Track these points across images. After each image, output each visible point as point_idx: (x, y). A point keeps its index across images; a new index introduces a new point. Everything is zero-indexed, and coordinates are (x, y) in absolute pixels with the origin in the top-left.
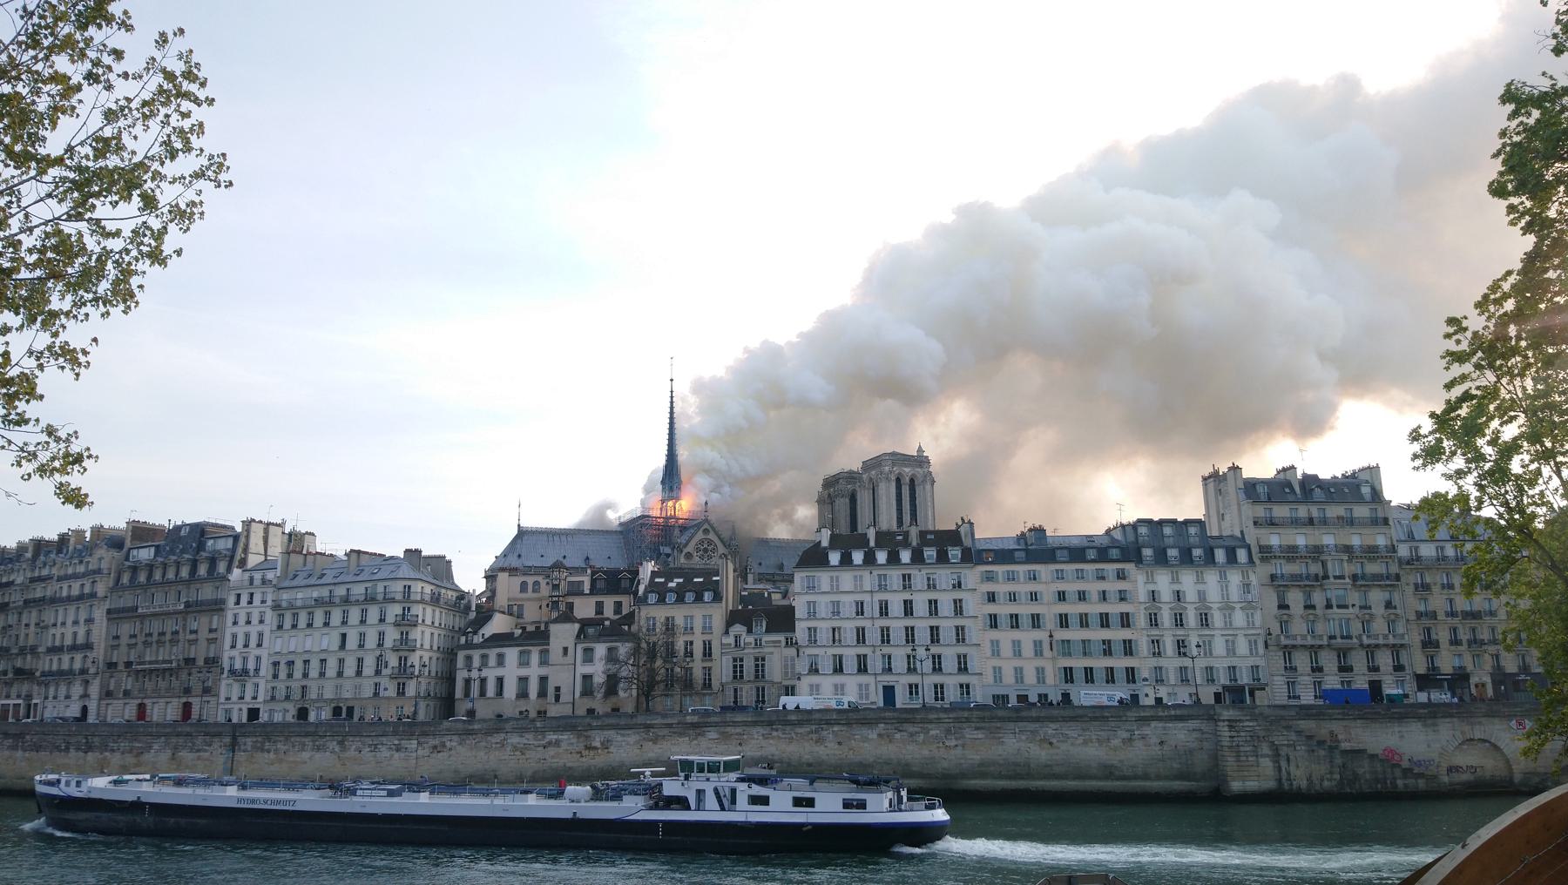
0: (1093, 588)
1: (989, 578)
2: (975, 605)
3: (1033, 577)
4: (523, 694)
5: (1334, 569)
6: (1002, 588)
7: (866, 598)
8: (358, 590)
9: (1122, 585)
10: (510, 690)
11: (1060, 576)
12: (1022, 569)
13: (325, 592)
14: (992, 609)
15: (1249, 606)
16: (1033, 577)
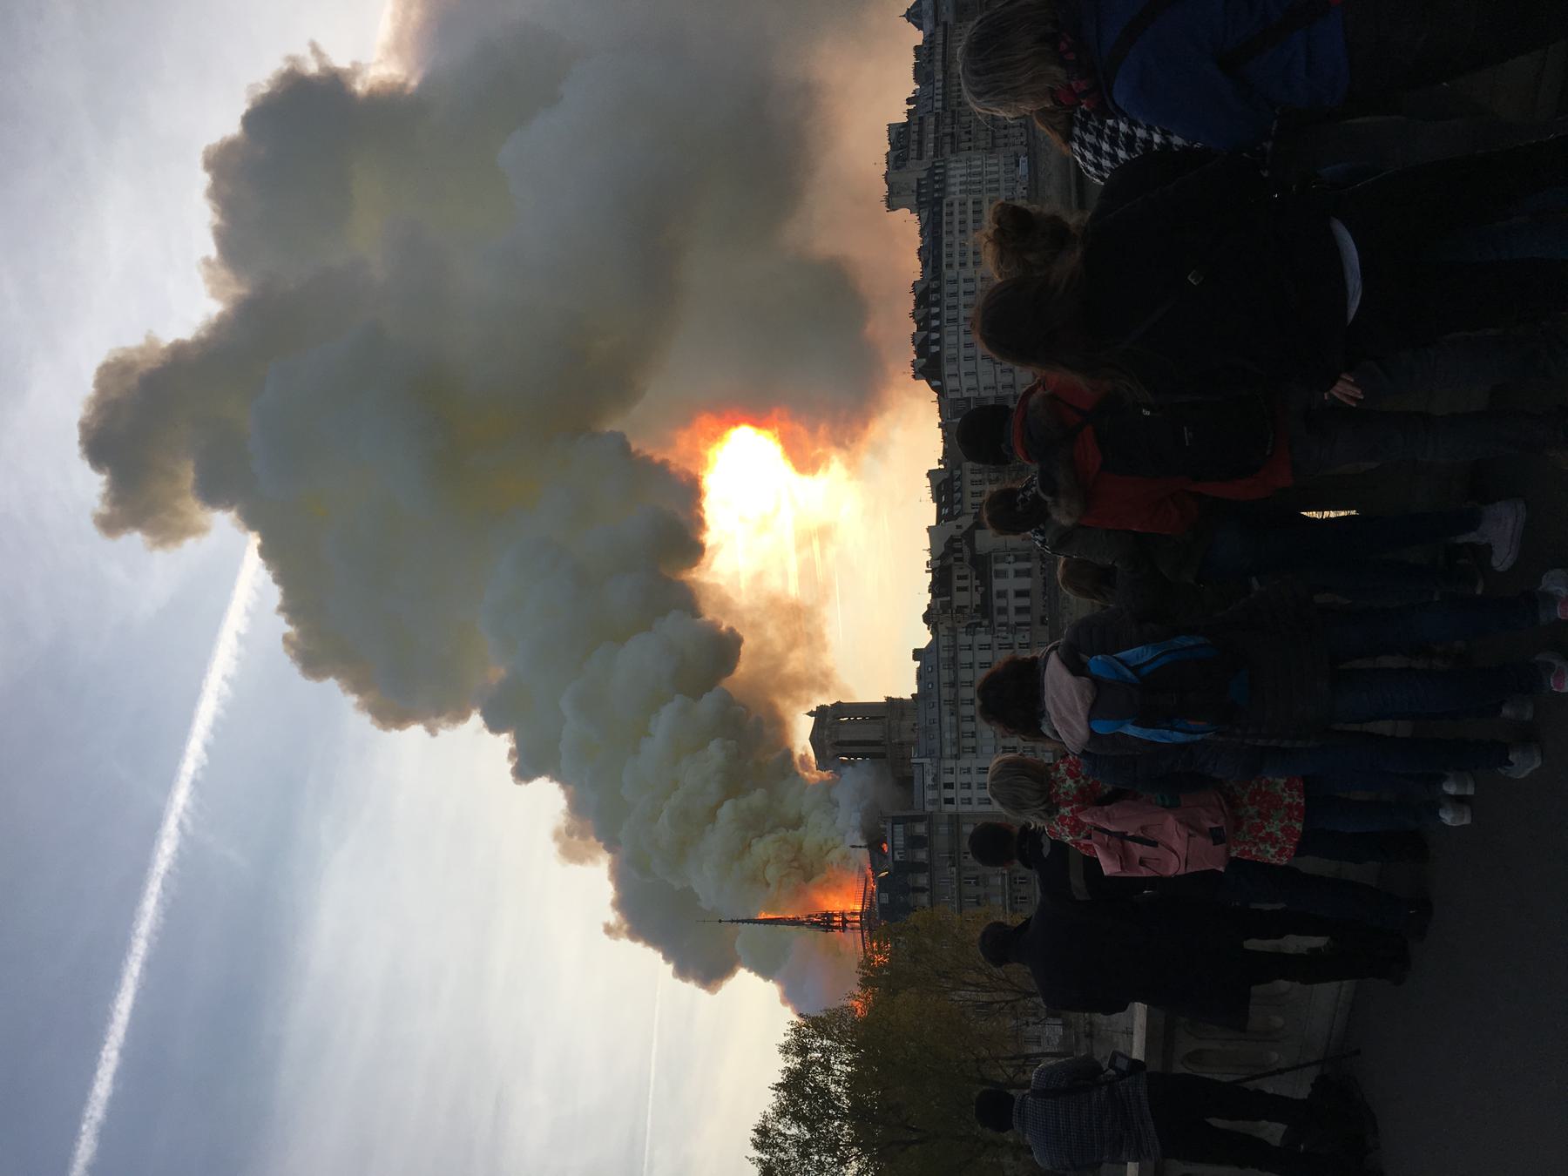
0: (957, 217)
1: (950, 266)
2: (969, 272)
3: (950, 245)
4: (1028, 573)
5: (948, 130)
6: (957, 259)
7: (962, 329)
8: (946, 675)
9: (956, 204)
10: (1025, 583)
11: (950, 233)
12: (945, 250)
13: (946, 709)
14: (970, 264)
15: (969, 159)
16: (950, 245)
